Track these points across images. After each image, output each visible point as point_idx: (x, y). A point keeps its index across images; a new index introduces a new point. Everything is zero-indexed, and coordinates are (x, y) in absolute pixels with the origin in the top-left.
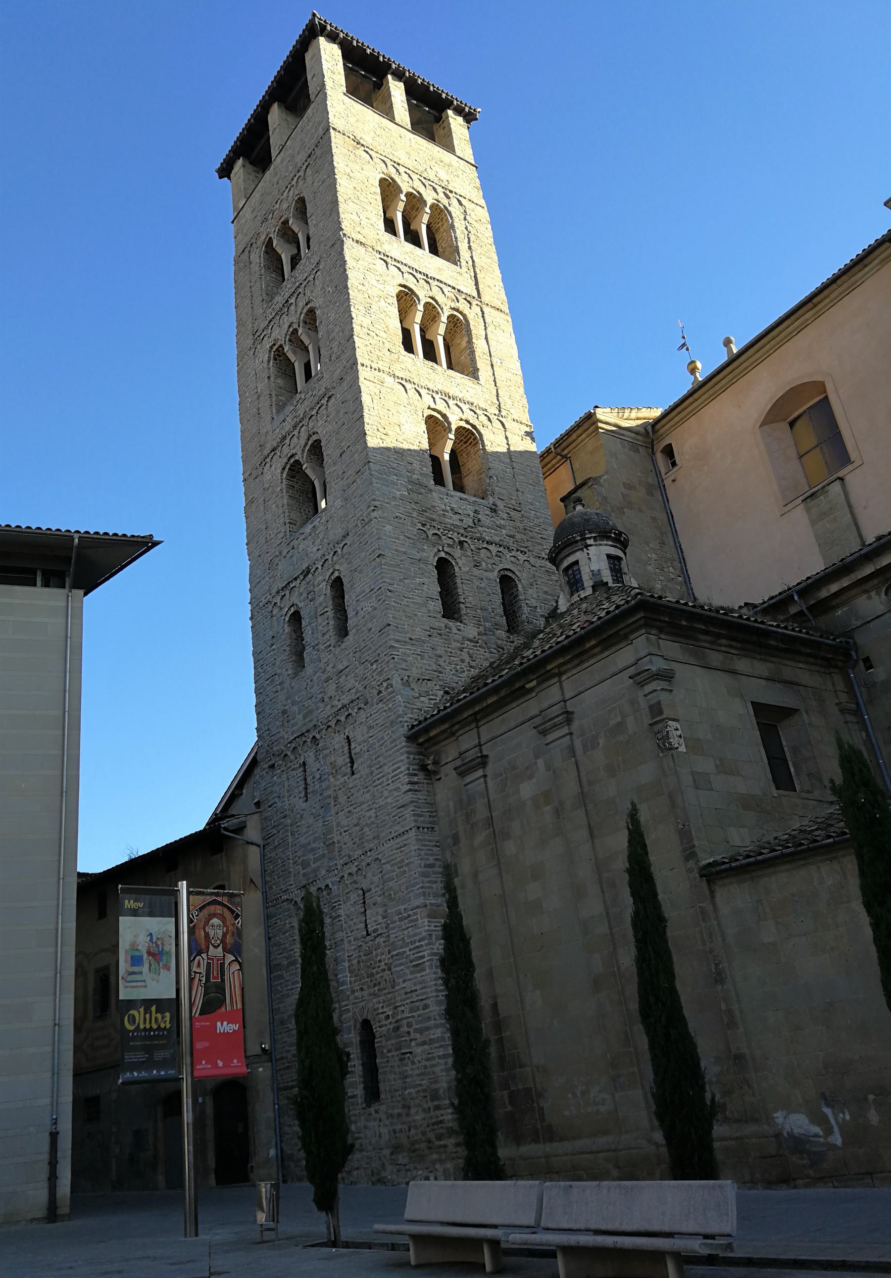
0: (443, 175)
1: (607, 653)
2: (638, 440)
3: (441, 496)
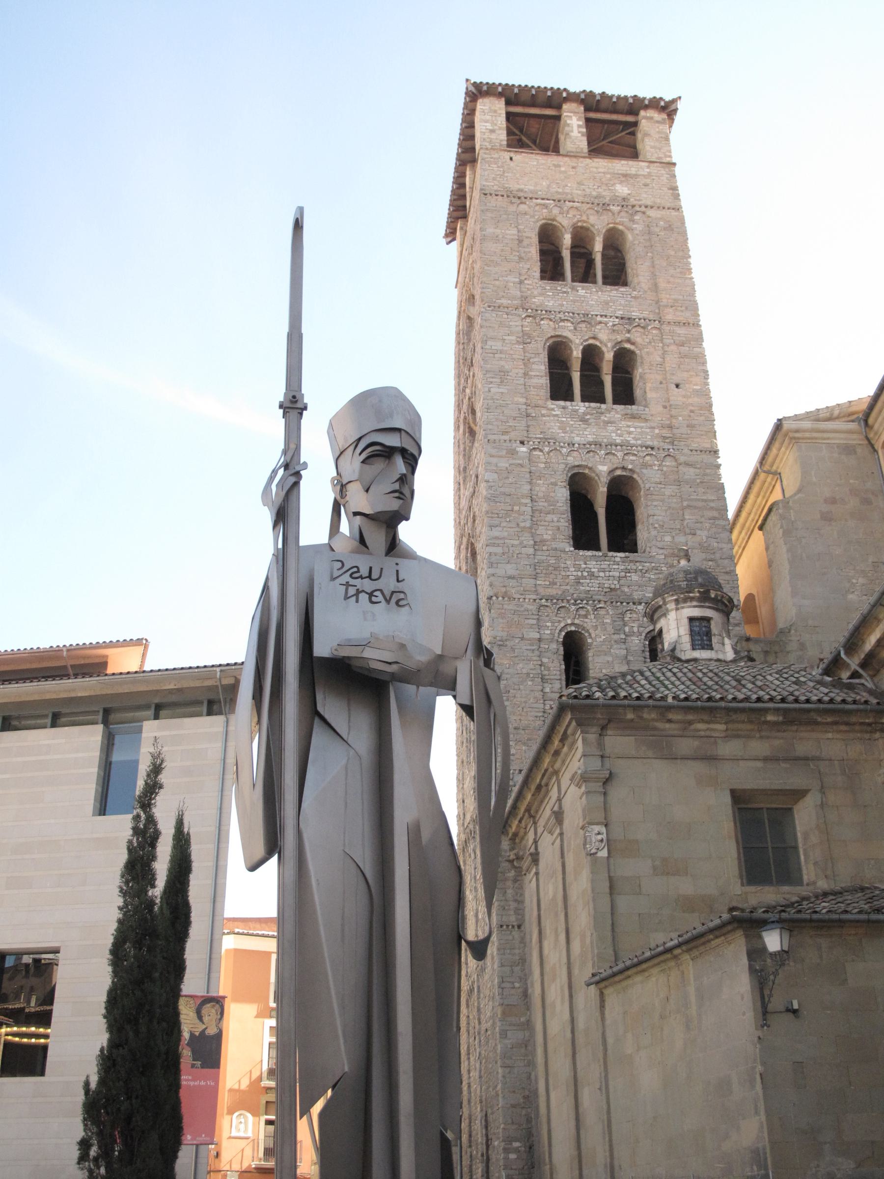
0: (622, 190)
1: (573, 752)
2: (854, 440)
3: (577, 563)
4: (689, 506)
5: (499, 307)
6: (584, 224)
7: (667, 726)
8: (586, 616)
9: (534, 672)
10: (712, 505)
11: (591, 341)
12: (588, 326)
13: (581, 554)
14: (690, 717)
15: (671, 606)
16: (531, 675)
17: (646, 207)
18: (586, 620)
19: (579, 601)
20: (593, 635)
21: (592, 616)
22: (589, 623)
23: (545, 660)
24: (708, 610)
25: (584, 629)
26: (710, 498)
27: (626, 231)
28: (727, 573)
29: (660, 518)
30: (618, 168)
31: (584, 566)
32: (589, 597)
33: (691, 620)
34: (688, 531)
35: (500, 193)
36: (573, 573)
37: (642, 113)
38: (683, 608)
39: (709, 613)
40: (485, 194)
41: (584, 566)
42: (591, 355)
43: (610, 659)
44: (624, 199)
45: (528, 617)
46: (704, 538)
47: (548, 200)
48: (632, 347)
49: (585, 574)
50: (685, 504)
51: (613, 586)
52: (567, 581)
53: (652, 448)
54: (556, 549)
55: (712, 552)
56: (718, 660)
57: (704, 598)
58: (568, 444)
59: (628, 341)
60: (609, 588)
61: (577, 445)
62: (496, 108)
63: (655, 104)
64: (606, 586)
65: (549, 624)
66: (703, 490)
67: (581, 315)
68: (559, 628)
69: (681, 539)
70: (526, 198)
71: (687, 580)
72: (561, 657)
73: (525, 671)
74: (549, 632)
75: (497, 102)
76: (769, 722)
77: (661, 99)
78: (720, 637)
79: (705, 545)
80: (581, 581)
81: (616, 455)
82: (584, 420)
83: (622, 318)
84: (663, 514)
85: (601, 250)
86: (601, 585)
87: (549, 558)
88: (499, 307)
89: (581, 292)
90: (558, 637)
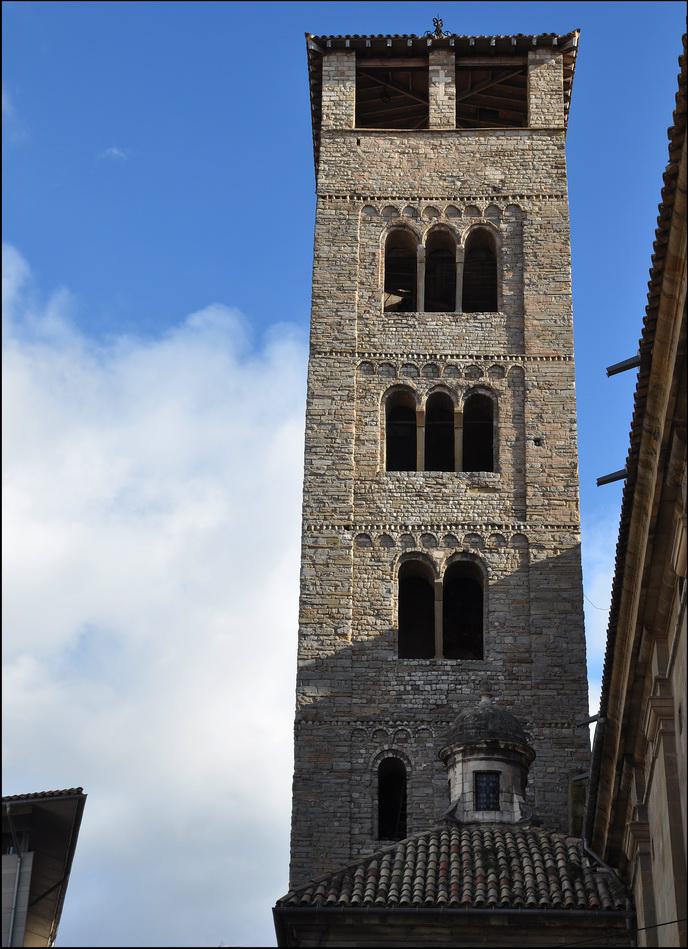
0: (494, 175)
4: (536, 599)
5: (331, 353)
6: (443, 229)
7: (389, 930)
8: (405, 740)
9: (341, 810)
10: (565, 595)
11: (437, 390)
12: (435, 370)
13: (405, 663)
14: (410, 922)
15: (459, 757)
16: (339, 815)
17: (522, 197)
18: (405, 745)
19: (398, 723)
20: (413, 763)
21: (413, 740)
22: (409, 748)
23: (356, 795)
24: (496, 763)
25: (403, 755)
26: (564, 586)
27: (494, 232)
28: (574, 681)
29: (501, 614)
30: (493, 142)
31: (408, 678)
32: (412, 716)
33: (477, 774)
34: (533, 630)
35: (341, 194)
36: (395, 687)
37: (531, 56)
38: (469, 760)
39: (496, 766)
40: (324, 197)
41: (408, 678)
42: (440, 402)
43: (430, 791)
44: (495, 189)
45: (340, 744)
46: (552, 637)
47: (400, 198)
48: (488, 394)
49: (409, 688)
50: (532, 595)
51: (439, 702)
52: (386, 697)
53: (500, 527)
54: (377, 659)
55: (560, 654)
56: (501, 823)
57: (492, 750)
58: (401, 528)
59: (482, 386)
60: (435, 704)
61: (410, 528)
62: (345, 69)
63: (546, 43)
64: (431, 701)
65: (363, 751)
66: (556, 577)
67: (428, 357)
68: (374, 755)
69: (524, 640)
70: (372, 198)
71: (477, 728)
72: (375, 790)
73: (331, 809)
74: (362, 761)
75: (346, 58)
76: (493, 927)
77: (553, 35)
78: (508, 795)
79: (552, 646)
80: (404, 697)
81: (455, 537)
82: (419, 495)
83: (478, 357)
84: (506, 609)
85: (463, 260)
86: (426, 701)
87: (368, 670)
88: (331, 353)
89: (432, 325)
90: (373, 766)
